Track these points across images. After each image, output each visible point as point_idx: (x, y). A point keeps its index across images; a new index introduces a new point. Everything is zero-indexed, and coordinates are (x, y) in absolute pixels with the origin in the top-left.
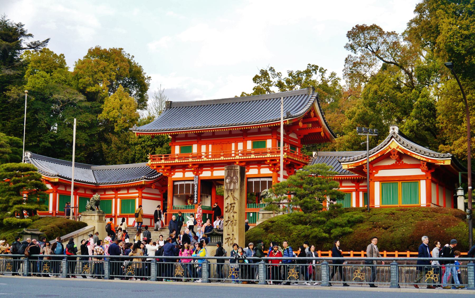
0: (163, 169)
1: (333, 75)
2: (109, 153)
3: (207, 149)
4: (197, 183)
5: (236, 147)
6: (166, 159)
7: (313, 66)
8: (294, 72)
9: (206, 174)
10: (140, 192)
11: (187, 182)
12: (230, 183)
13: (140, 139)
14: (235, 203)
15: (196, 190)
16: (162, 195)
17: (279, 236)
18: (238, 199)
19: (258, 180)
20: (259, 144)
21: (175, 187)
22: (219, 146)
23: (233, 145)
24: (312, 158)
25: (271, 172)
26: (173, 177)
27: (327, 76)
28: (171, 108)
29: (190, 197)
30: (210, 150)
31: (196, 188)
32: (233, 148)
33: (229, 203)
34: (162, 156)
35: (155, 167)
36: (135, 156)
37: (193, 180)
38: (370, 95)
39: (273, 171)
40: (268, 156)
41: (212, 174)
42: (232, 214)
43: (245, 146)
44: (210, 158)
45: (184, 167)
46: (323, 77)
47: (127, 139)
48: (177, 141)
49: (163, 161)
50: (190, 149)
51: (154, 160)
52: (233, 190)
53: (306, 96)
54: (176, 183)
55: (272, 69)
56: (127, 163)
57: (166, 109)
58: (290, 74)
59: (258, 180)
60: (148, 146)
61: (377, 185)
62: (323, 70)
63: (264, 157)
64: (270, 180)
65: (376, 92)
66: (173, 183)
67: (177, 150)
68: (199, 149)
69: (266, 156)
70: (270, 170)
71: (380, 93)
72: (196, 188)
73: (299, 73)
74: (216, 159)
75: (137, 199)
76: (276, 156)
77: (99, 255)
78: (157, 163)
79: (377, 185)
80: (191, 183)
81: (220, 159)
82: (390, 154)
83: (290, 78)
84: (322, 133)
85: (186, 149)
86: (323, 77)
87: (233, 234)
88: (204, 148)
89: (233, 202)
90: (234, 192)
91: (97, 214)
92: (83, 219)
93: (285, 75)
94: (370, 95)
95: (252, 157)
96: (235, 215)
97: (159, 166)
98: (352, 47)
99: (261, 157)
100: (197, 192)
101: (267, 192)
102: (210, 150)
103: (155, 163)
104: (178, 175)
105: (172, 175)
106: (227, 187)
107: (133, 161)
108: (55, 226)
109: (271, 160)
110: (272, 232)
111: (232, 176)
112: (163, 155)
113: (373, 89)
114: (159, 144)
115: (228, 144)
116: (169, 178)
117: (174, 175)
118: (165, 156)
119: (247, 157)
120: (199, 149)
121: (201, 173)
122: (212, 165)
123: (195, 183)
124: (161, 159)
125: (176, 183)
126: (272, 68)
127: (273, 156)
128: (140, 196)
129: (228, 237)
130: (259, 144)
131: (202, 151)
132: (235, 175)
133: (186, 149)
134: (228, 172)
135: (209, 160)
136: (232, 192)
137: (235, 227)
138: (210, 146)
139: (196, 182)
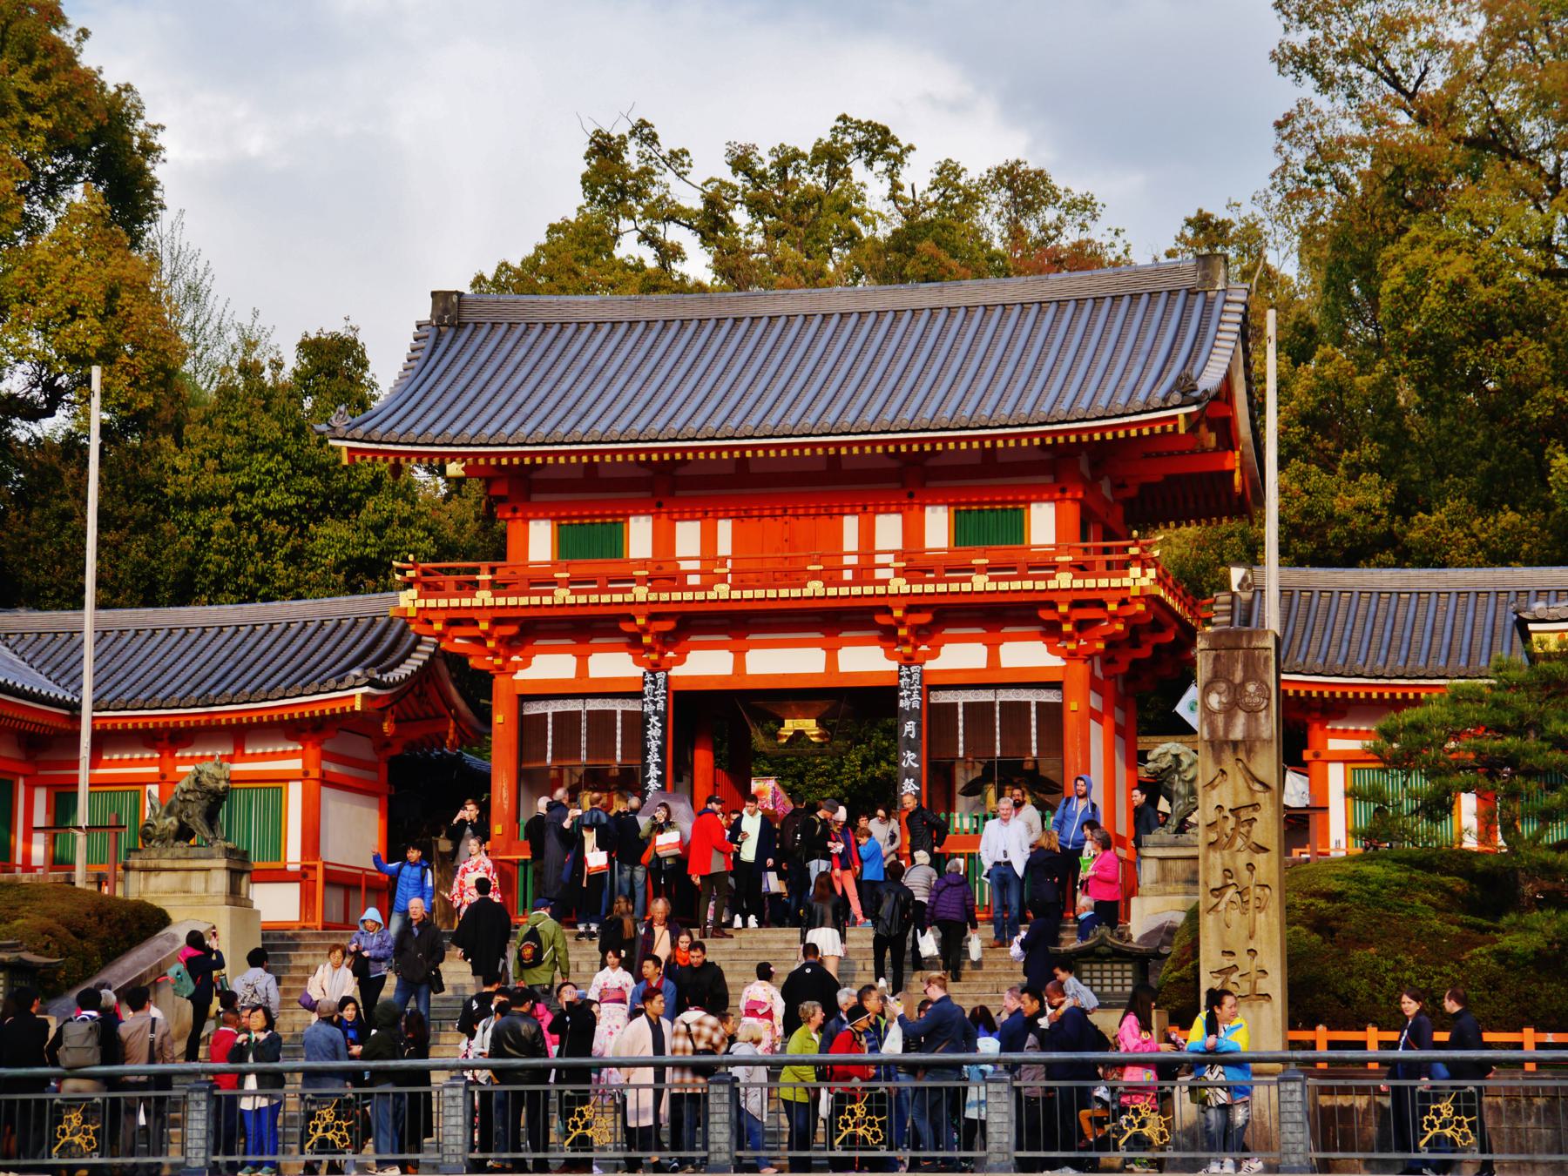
0: (479, 640)
1: (948, 174)
2: (39, 542)
3: (709, 540)
4: (660, 707)
5: (867, 535)
6: (497, 587)
7: (859, 126)
8: (763, 152)
9: (706, 664)
10: (313, 753)
12: (1229, 711)
13: (227, 479)
14: (1255, 806)
15: (653, 745)
16: (384, 768)
17: (1410, 961)
18: (1274, 784)
20: (987, 526)
21: (529, 729)
22: (772, 529)
23: (851, 525)
24: (1223, 597)
25: (1057, 661)
26: (521, 675)
27: (918, 176)
28: (461, 326)
29: (615, 779)
30: (724, 547)
31: (654, 732)
32: (851, 540)
33: (1228, 805)
34: (476, 571)
35: (438, 627)
36: (194, 561)
37: (639, 695)
38: (1432, 302)
39: (1070, 656)
40: (1065, 584)
41: (739, 664)
42: (1243, 859)
43: (913, 533)
44: (694, 589)
45: (581, 630)
46: (896, 187)
47: (150, 473)
48: (536, 498)
49: (484, 597)
50: (616, 543)
51: (429, 589)
52: (1247, 746)
53: (1200, 299)
54: (533, 709)
55: (645, 133)
56: (150, 601)
57: (432, 333)
58: (742, 162)
60: (267, 513)
62: (894, 149)
63: (1040, 585)
64: (1050, 697)
65: (1458, 289)
66: (520, 709)
67: (540, 541)
68: (665, 541)
69: (1052, 585)
71: (1483, 293)
72: (654, 732)
73: (787, 159)
74: (784, 593)
75: (295, 791)
76: (1103, 583)
77: (706, 1052)
78: (454, 602)
80: (618, 706)
81: (807, 592)
83: (739, 180)
84: (1237, 477)
85: (589, 542)
86: (896, 187)
87: (1252, 952)
88: (688, 536)
89: (1244, 799)
90: (1250, 752)
91: (223, 863)
92: (137, 888)
93: (711, 166)
94: (1432, 302)
95: (979, 587)
96: (1259, 860)
97: (456, 621)
98: (1304, 62)
99: (1028, 585)
100: (662, 751)
101: (1176, 756)
102: (724, 547)
103: (443, 603)
104: (550, 666)
105: (518, 666)
106: (1213, 730)
107: (184, 595)
108: (51, 922)
109: (1075, 605)
110: (1361, 942)
111: (1238, 676)
112: (485, 565)
113: (1451, 275)
114: (324, 507)
115: (823, 521)
116: (500, 682)
117: (526, 664)
118: (492, 571)
119: (954, 587)
120: (665, 541)
121: (681, 660)
122: (737, 625)
123: (649, 708)
124: (476, 586)
125: (533, 709)
126: (644, 124)
127: (1090, 583)
128: (315, 773)
129: (1227, 962)
130: (987, 526)
131: (680, 552)
132: (1252, 672)
133: (589, 542)
134: (1217, 658)
135: (844, 591)
136: (1242, 756)
137: (1261, 917)
138: (725, 528)
139: (655, 704)
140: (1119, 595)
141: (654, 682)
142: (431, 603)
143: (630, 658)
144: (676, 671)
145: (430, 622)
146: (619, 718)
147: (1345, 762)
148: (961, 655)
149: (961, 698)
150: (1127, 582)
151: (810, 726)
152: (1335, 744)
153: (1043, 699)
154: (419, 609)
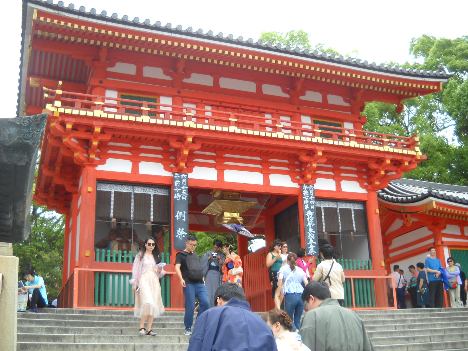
9: (204, 174)
19: (332, 205)
21: (102, 199)
25: (364, 191)
26: (100, 168)
35: (69, 126)
54: (104, 188)
59: (332, 205)
64: (359, 207)
70: (362, 186)
80: (152, 192)
103: (76, 112)
104: (117, 166)
125: (104, 188)
140: (409, 159)
141: (181, 180)
142: (68, 111)
143: (162, 166)
144: (191, 176)
145: (63, 124)
146: (152, 198)
147: (449, 246)
148: (325, 185)
149: (323, 205)
150: (413, 153)
151: (236, 215)
152: (444, 239)
153: (356, 208)
154: (61, 114)
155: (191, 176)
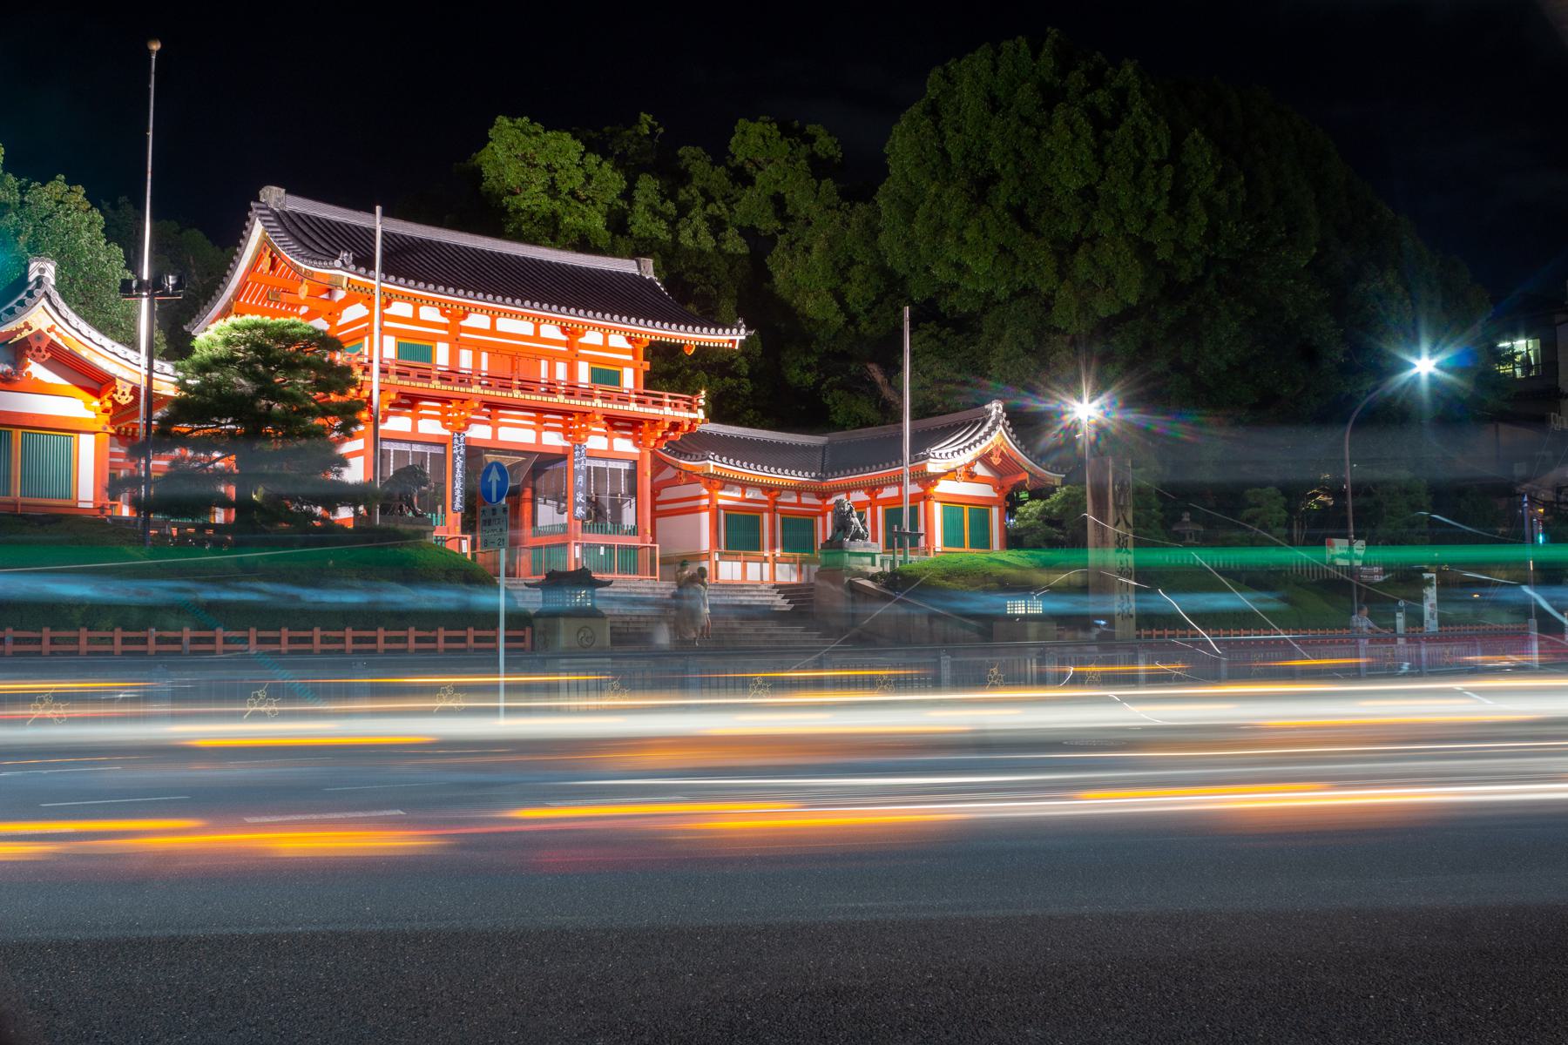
9: (480, 432)
11: (417, 448)
19: (602, 464)
23: (544, 364)
32: (544, 374)
54: (386, 446)
59: (602, 464)
61: (937, 509)
70: (636, 445)
79: (937, 509)
80: (429, 450)
82: (990, 454)
138: (485, 356)
139: (458, 450)
144: (468, 434)
148: (597, 442)
155: (468, 434)
